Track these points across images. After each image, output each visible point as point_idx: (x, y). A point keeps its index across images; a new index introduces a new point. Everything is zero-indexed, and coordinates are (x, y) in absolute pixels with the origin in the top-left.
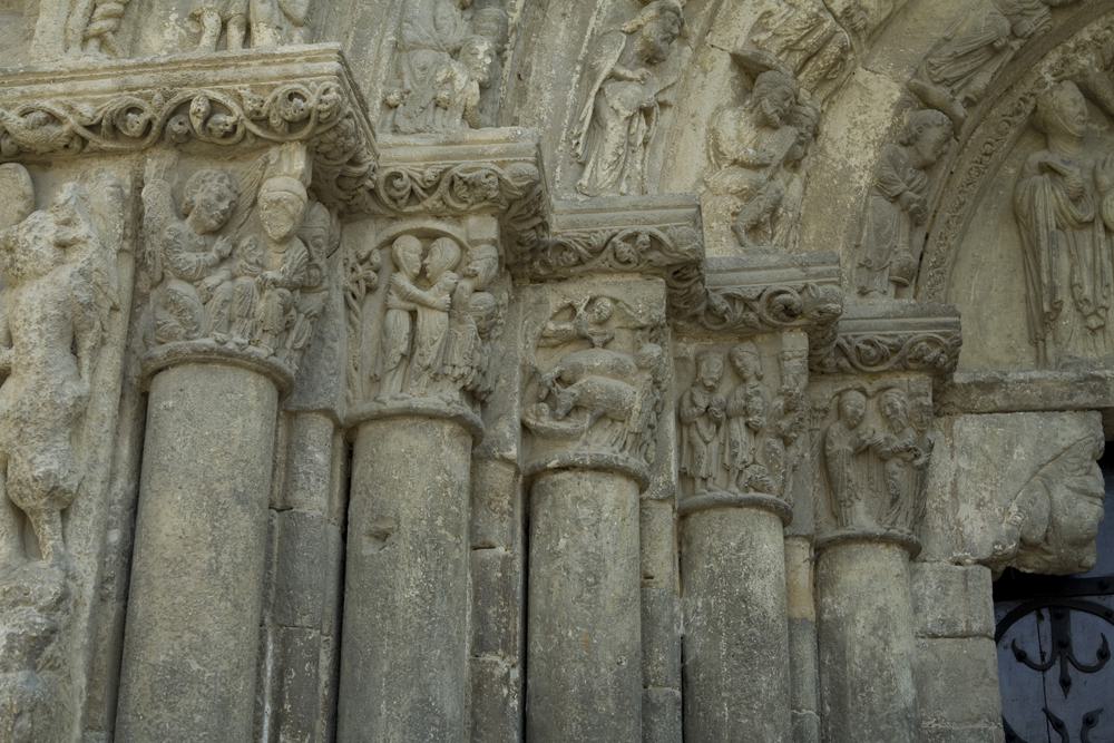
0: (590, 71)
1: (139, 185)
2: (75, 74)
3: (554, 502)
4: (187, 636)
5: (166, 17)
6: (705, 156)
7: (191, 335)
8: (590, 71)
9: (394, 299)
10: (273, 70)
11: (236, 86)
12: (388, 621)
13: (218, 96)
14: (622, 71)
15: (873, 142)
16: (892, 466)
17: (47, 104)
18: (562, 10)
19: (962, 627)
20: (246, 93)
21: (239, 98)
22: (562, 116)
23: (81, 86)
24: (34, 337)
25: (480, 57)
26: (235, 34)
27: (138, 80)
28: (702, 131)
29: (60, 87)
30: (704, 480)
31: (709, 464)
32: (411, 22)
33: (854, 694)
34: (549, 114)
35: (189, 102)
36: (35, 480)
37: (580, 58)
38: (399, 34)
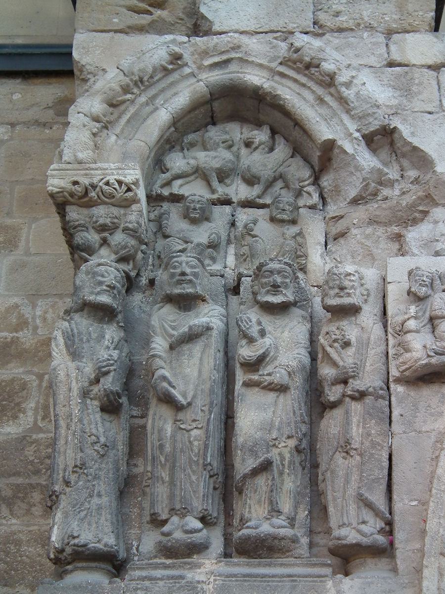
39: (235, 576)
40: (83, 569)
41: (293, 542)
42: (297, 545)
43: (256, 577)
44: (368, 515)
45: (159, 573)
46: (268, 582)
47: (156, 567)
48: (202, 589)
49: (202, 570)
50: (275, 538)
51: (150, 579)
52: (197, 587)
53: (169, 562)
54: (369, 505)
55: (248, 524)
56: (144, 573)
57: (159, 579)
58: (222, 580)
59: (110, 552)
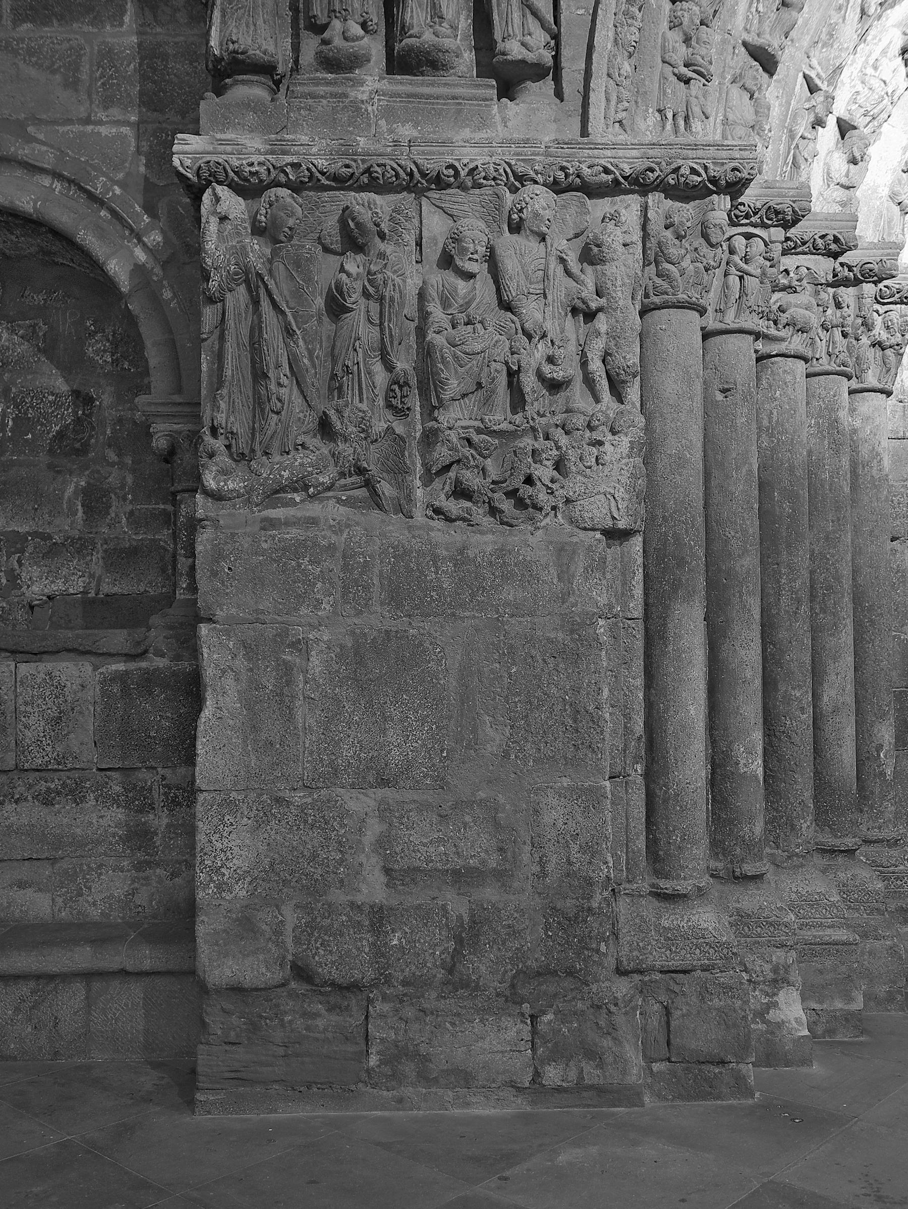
0: (792, 135)
1: (645, 209)
2: (614, 146)
3: (772, 371)
4: (684, 441)
5: (647, 110)
6: (822, 178)
7: (676, 293)
8: (792, 135)
9: (733, 270)
10: (724, 154)
11: (705, 161)
12: (734, 433)
13: (695, 166)
14: (806, 135)
15: (891, 169)
16: (889, 352)
17: (603, 162)
18: (776, 94)
19: (901, 435)
20: (711, 166)
21: (706, 168)
22: (778, 160)
23: (621, 153)
24: (619, 294)
25: (766, 132)
26: (681, 123)
27: (651, 153)
28: (822, 164)
29: (608, 153)
30: (817, 359)
31: (821, 352)
32: (731, 109)
33: (863, 467)
34: (771, 158)
35: (680, 167)
36: (628, 367)
37: (786, 125)
38: (725, 116)
39: (399, 96)
40: (243, 82)
41: (457, 57)
42: (461, 61)
43: (420, 98)
44: (533, 24)
45: (322, 89)
46: (433, 104)
47: (317, 82)
48: (366, 110)
49: (365, 88)
50: (440, 50)
51: (313, 96)
52: (361, 108)
53: (330, 76)
54: (535, 14)
55: (411, 32)
56: (306, 89)
57: (322, 97)
58: (388, 101)
59: (269, 62)
